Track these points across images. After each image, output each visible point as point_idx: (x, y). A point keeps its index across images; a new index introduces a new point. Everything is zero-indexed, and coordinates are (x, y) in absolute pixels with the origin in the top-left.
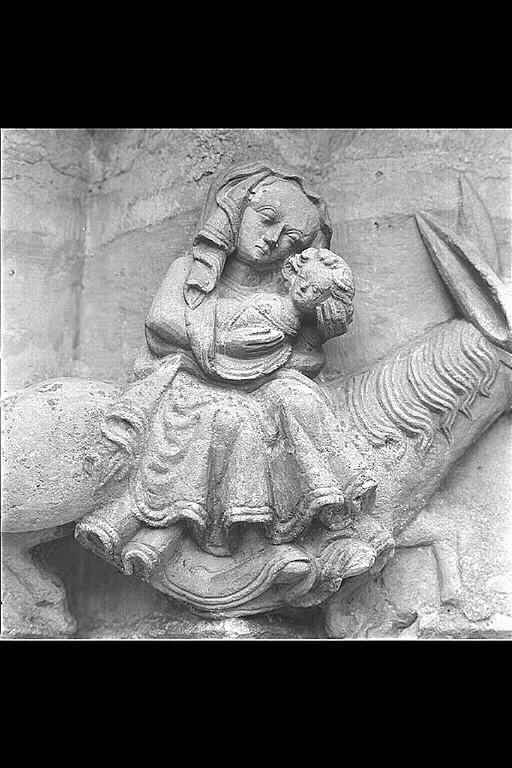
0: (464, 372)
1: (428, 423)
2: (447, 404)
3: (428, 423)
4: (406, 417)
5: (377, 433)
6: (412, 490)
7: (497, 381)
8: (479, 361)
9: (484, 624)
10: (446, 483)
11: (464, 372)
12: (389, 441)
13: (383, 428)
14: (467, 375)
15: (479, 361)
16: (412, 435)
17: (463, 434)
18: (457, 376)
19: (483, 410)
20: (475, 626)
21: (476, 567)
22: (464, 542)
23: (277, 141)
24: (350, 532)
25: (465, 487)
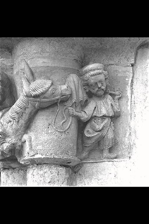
0: (21, 104)
1: (16, 116)
2: (19, 111)
3: (16, 116)
4: (12, 116)
5: (8, 120)
6: (17, 131)
7: (29, 104)
8: (24, 101)
9: (32, 157)
10: (27, 127)
11: (21, 104)
12: (10, 121)
13: (8, 119)
14: (22, 104)
15: (24, 101)
16: (14, 119)
17: (26, 117)
18: (20, 105)
19: (28, 111)
20: (31, 158)
21: (35, 145)
22: (32, 140)
23: (3, 62)
24: (5, 142)
25: (33, 127)
